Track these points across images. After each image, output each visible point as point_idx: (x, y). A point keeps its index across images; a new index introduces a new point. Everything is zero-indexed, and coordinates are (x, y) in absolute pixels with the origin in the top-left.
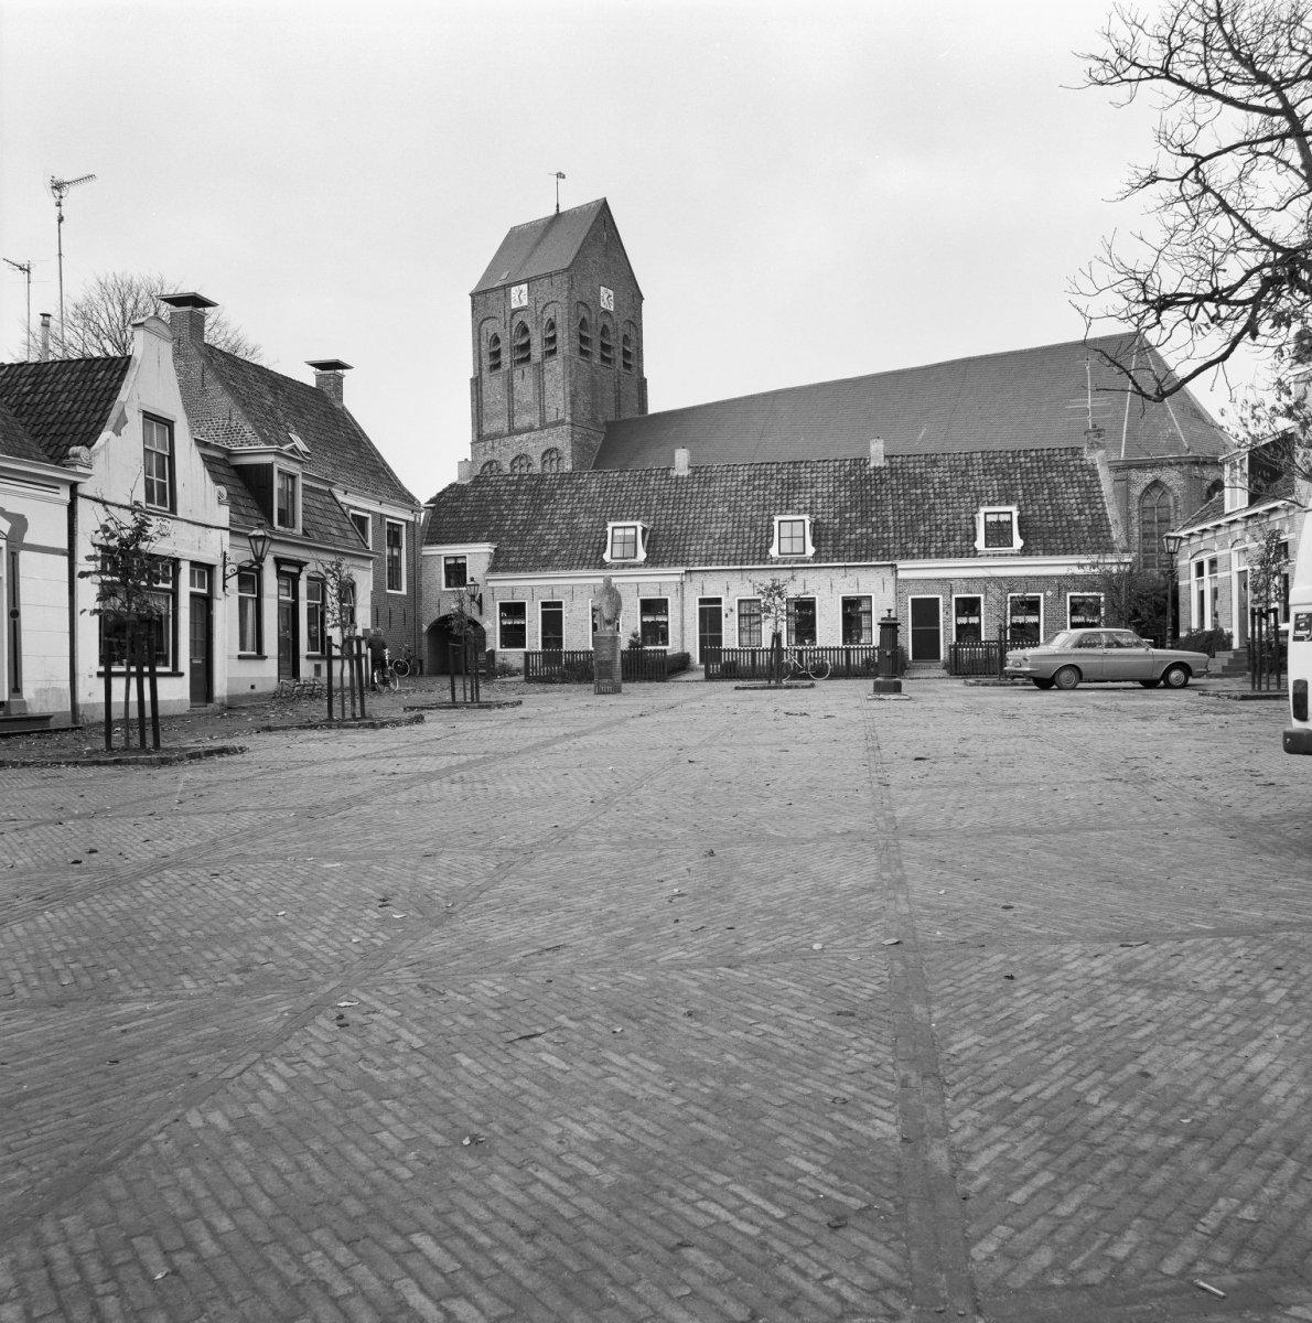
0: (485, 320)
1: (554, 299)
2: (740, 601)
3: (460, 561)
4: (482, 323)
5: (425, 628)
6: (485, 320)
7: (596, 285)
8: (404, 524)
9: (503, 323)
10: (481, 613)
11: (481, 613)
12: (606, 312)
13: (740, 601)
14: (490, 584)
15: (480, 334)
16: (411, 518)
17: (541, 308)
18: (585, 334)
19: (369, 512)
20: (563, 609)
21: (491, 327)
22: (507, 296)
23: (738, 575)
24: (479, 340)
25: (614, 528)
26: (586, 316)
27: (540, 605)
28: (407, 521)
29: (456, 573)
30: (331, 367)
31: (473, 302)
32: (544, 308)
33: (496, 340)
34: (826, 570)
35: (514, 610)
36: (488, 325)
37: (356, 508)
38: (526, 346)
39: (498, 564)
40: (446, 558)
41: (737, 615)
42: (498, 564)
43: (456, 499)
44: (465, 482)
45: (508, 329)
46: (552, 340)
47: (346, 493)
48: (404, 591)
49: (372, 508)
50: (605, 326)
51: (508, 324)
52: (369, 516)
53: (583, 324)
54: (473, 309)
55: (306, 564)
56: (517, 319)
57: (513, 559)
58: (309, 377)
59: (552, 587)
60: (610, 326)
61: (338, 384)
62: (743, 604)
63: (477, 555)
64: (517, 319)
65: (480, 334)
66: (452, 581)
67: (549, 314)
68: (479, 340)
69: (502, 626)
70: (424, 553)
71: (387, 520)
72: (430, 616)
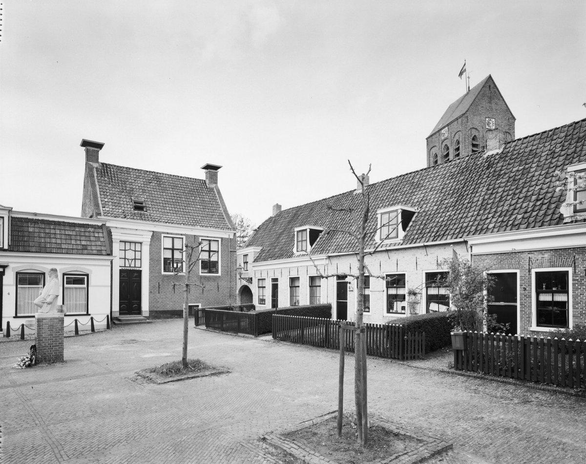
1: (459, 130)
6: (431, 148)
18: (475, 143)
19: (182, 235)
21: (434, 151)
26: (477, 134)
30: (212, 169)
31: (427, 141)
33: (436, 156)
34: (414, 251)
36: (433, 150)
38: (447, 155)
45: (440, 149)
46: (458, 149)
49: (184, 233)
55: (7, 266)
56: (444, 144)
58: (202, 175)
61: (213, 178)
64: (444, 144)
66: (125, 274)
67: (457, 137)
72: (239, 287)
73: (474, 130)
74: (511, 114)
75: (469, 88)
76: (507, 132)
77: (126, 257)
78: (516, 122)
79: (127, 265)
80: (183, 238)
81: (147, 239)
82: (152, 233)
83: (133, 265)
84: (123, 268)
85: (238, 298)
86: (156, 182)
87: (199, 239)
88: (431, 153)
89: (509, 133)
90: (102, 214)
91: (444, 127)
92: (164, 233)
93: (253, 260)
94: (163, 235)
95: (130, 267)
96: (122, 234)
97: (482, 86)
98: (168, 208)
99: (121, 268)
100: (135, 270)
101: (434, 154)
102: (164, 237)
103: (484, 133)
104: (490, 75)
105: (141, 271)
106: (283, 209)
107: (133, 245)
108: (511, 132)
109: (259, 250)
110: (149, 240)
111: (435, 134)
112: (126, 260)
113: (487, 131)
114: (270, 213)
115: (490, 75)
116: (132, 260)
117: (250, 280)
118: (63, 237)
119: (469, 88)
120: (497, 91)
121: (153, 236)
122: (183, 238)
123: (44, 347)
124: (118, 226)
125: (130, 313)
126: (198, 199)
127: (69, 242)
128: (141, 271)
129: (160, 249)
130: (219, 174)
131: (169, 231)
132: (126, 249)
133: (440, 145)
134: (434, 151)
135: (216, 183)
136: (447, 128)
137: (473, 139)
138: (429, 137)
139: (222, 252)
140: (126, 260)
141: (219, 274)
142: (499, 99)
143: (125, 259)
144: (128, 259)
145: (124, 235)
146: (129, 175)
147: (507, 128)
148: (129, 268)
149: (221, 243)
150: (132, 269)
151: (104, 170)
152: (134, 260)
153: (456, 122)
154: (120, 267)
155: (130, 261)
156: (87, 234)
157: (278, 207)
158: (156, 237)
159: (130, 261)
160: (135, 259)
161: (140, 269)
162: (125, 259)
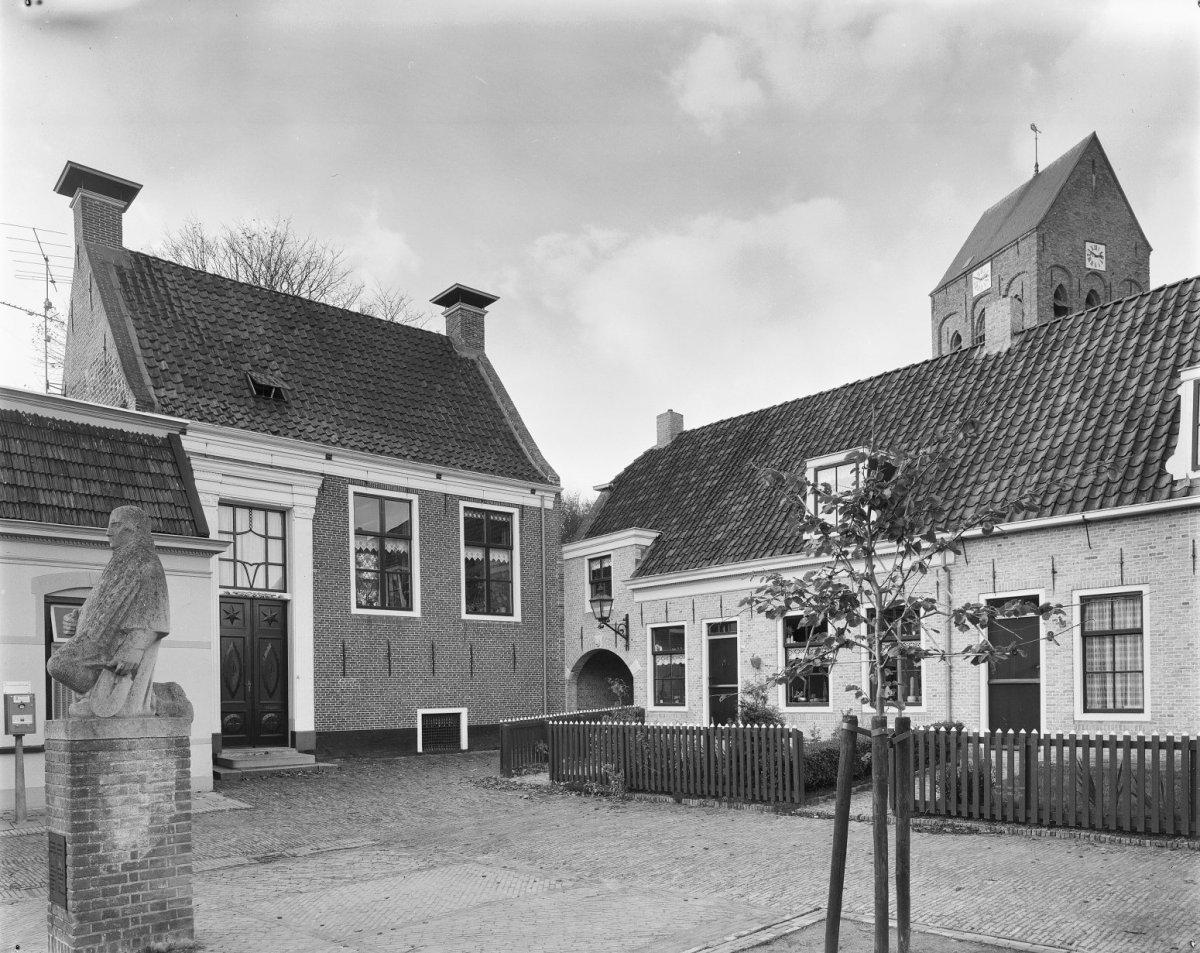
0: (945, 319)
1: (1021, 270)
2: (1086, 601)
3: (606, 565)
4: (942, 323)
5: (568, 673)
6: (945, 319)
7: (1078, 242)
8: (516, 512)
9: (964, 316)
10: (627, 647)
11: (627, 647)
12: (1095, 273)
13: (1086, 601)
14: (639, 597)
15: (940, 337)
16: (533, 501)
17: (1005, 287)
18: (1061, 304)
19: (408, 490)
20: (738, 636)
21: (951, 326)
22: (968, 284)
23: (1078, 537)
24: (940, 343)
25: (817, 470)
26: (1065, 282)
27: (705, 629)
28: (522, 508)
29: (601, 581)
31: (933, 302)
32: (1009, 284)
35: (669, 639)
37: (366, 484)
39: (652, 564)
40: (591, 560)
41: (1077, 631)
42: (652, 564)
43: (642, 472)
44: (662, 446)
47: (439, 476)
48: (517, 617)
50: (1092, 291)
51: (970, 316)
52: (414, 498)
53: (1059, 293)
54: (933, 309)
57: (671, 552)
59: (720, 596)
60: (1100, 291)
61: (474, 330)
62: (1095, 608)
63: (625, 546)
65: (940, 337)
68: (940, 343)
69: (657, 669)
70: (566, 556)
71: (463, 504)
72: (573, 654)
73: (1057, 272)
74: (1142, 235)
75: (1037, 165)
76: (1132, 281)
77: (239, 558)
78: (1153, 257)
79: (242, 582)
80: (410, 502)
81: (303, 501)
82: (318, 482)
83: (260, 583)
84: (231, 592)
85: (570, 693)
86: (308, 327)
87: (457, 505)
88: (944, 332)
89: (1136, 283)
90: (157, 405)
91: (981, 264)
92: (355, 482)
93: (632, 568)
94: (352, 489)
95: (251, 588)
96: (225, 479)
97: (1075, 161)
98: (356, 408)
99: (222, 592)
100: (268, 599)
101: (951, 335)
102: (355, 494)
103: (1082, 280)
104: (1094, 133)
105: (285, 603)
106: (688, 426)
107: (259, 516)
108: (1141, 280)
109: (648, 542)
110: (313, 502)
111: (954, 281)
112: (239, 565)
113: (1087, 275)
114: (648, 439)
115: (1094, 133)
116: (259, 565)
117: (624, 633)
118: (38, 466)
119: (1037, 165)
120: (1110, 176)
121: (322, 489)
122: (410, 502)
123: (104, 881)
124: (212, 450)
125: (669, 702)
126: (439, 387)
127: (58, 483)
128: (285, 603)
129: (346, 533)
130: (486, 318)
131: (372, 477)
132: (238, 530)
133: (969, 310)
134: (951, 326)
135: (481, 347)
136: (987, 267)
137: (1057, 296)
138: (938, 291)
139: (522, 549)
140: (239, 564)
141: (517, 617)
142: (1115, 197)
143: (235, 561)
144: (243, 563)
145: (245, 482)
146: (224, 299)
147: (1131, 270)
148: (250, 593)
149: (521, 523)
150: (258, 594)
151: (142, 273)
152: (262, 568)
153: (1012, 252)
154: (221, 587)
155: (251, 570)
156: (121, 462)
157: (675, 418)
158: (331, 490)
159: (251, 570)
160: (267, 564)
161: (286, 596)
162: (235, 561)
